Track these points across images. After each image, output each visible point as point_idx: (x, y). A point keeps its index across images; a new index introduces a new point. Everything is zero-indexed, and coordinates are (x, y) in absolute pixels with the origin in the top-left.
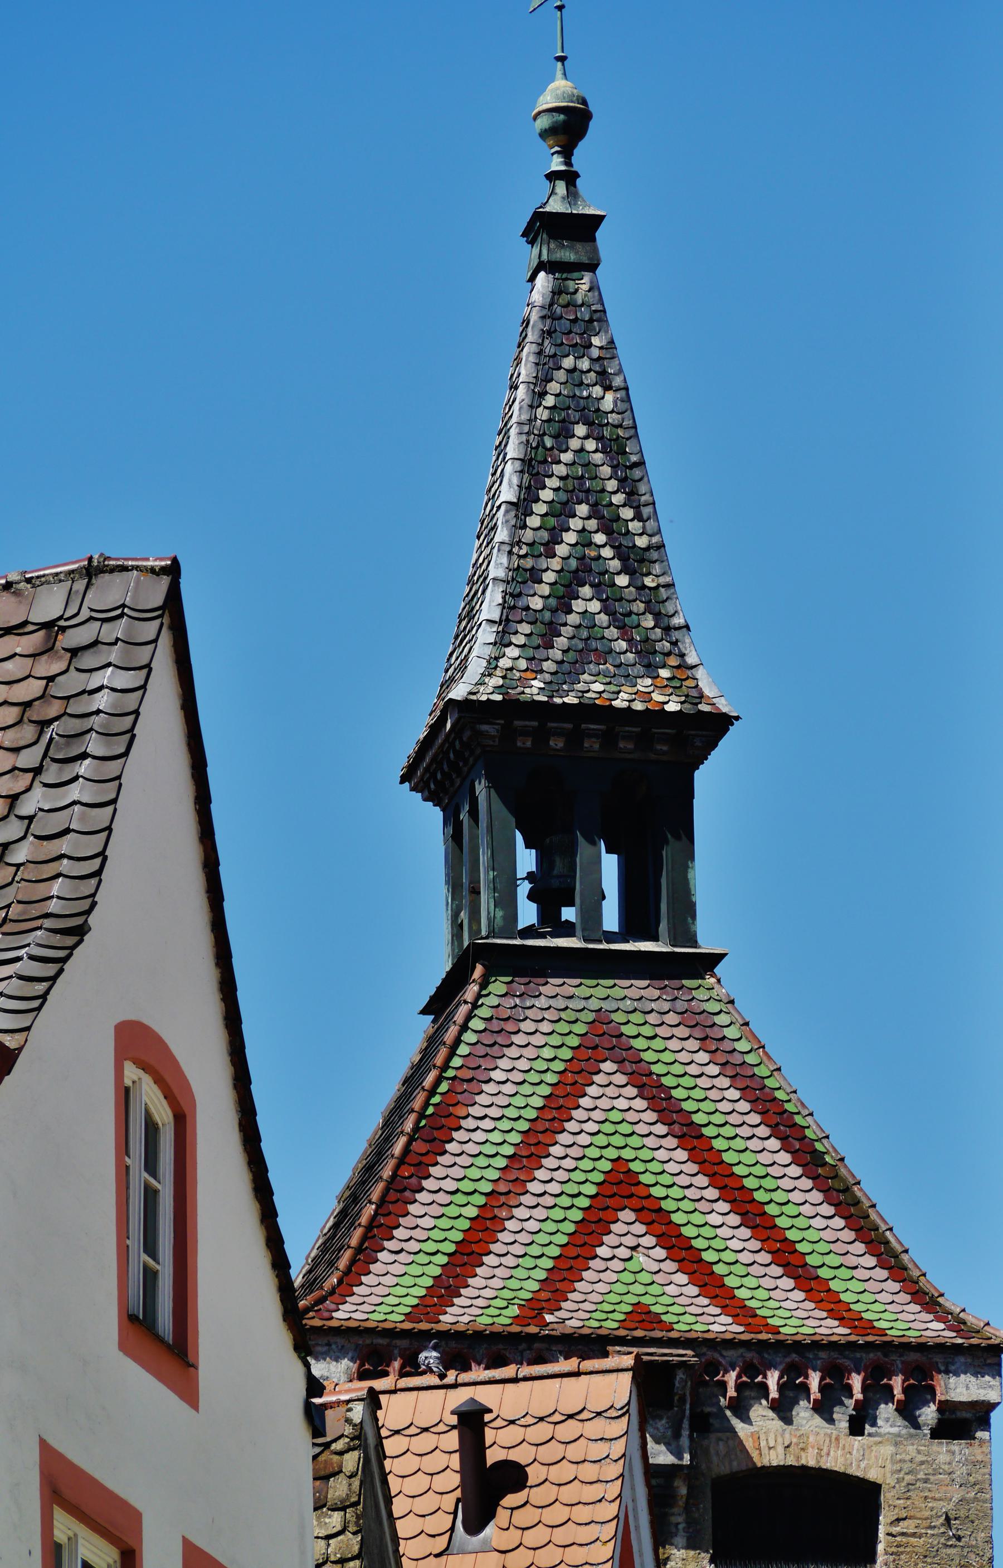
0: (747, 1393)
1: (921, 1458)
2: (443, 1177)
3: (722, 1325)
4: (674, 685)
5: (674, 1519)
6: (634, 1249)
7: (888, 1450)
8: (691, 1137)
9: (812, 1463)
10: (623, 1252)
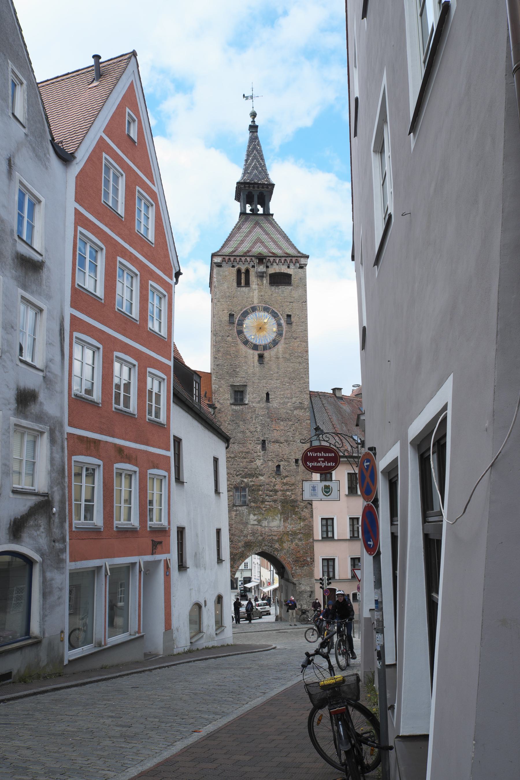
4: (267, 181)
7: (292, 270)
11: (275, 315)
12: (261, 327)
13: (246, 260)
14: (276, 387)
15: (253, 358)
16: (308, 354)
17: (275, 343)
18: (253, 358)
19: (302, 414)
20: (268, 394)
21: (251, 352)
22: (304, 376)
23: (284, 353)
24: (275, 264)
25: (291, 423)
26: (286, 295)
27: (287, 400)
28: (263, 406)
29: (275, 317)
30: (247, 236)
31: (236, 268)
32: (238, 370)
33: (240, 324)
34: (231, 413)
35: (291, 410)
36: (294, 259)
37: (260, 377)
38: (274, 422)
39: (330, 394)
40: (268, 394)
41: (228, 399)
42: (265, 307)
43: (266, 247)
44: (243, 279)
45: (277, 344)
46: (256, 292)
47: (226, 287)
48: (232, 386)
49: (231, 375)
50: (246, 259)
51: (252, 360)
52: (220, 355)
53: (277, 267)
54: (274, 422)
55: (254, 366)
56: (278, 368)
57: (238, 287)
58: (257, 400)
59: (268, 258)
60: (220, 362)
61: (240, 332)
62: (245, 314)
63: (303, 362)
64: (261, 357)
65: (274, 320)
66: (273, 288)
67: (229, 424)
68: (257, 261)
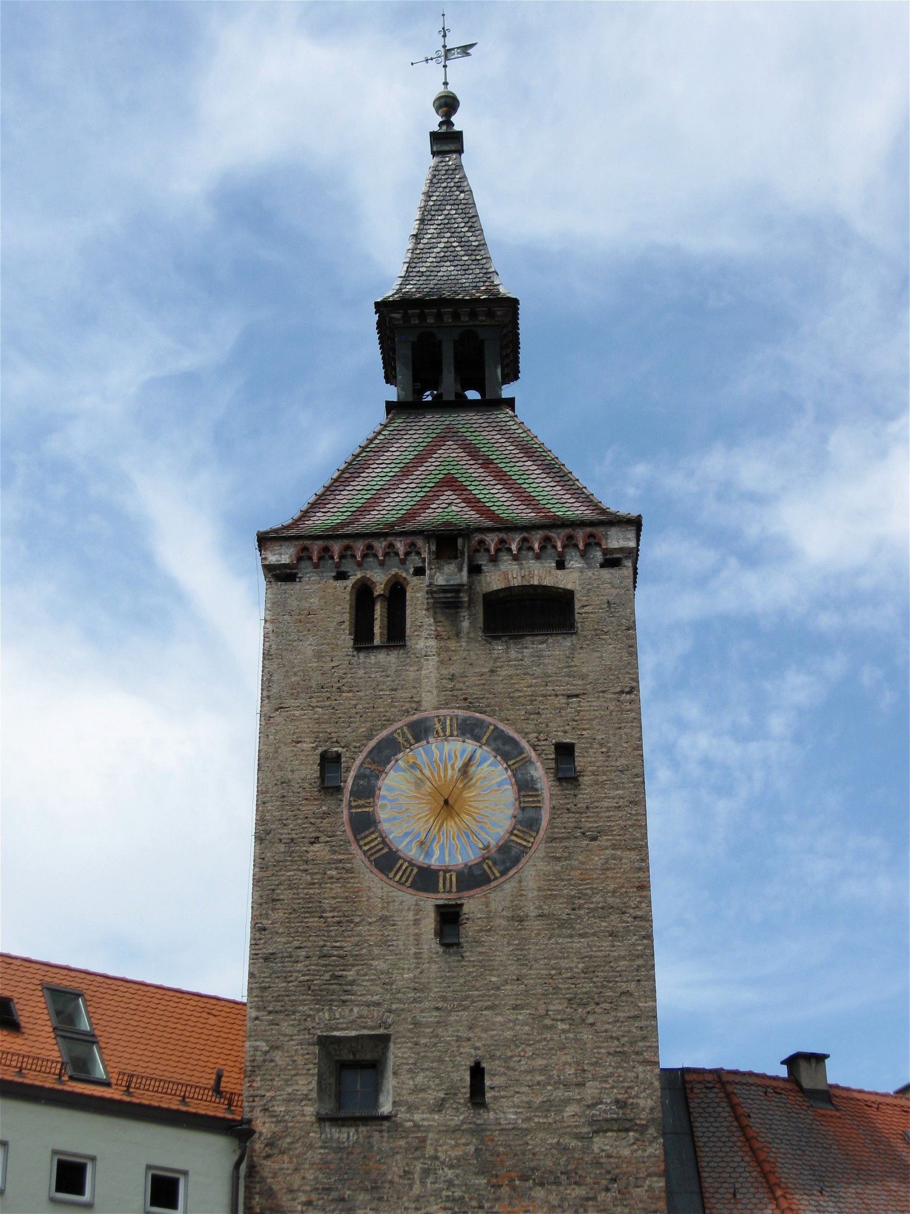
0: (501, 554)
1: (595, 577)
2: (358, 484)
3: (489, 524)
6: (449, 504)
7: (576, 575)
8: (487, 463)
9: (536, 583)
10: (444, 506)
11: (507, 749)
12: (446, 801)
13: (391, 551)
14: (515, 1041)
16: (647, 900)
17: (507, 857)
18: (417, 922)
19: (626, 1152)
20: (477, 1072)
21: (408, 897)
22: (632, 986)
23: (548, 896)
24: (505, 557)
25: (580, 1191)
26: (550, 669)
27: (560, 1094)
28: (457, 1120)
29: (506, 757)
30: (406, 471)
31: (349, 583)
32: (351, 974)
33: (366, 790)
34: (315, 1155)
35: (579, 1137)
36: (580, 535)
37: (444, 999)
38: (505, 1191)
39: (776, 1078)
40: (477, 1072)
41: (306, 1097)
42: (465, 720)
43: (473, 502)
44: (377, 620)
45: (516, 861)
46: (430, 667)
47: (309, 652)
48: (325, 1043)
49: (322, 998)
50: (391, 546)
51: (412, 930)
52: (280, 915)
53: (515, 567)
54: (505, 1191)
55: (418, 956)
56: (522, 961)
57: (358, 649)
58: (432, 1096)
59: (478, 537)
60: (279, 944)
61: (364, 823)
62: (385, 753)
63: (627, 930)
64: (449, 919)
65: (501, 768)
66: (499, 648)
67: (309, 1203)
68: (434, 548)
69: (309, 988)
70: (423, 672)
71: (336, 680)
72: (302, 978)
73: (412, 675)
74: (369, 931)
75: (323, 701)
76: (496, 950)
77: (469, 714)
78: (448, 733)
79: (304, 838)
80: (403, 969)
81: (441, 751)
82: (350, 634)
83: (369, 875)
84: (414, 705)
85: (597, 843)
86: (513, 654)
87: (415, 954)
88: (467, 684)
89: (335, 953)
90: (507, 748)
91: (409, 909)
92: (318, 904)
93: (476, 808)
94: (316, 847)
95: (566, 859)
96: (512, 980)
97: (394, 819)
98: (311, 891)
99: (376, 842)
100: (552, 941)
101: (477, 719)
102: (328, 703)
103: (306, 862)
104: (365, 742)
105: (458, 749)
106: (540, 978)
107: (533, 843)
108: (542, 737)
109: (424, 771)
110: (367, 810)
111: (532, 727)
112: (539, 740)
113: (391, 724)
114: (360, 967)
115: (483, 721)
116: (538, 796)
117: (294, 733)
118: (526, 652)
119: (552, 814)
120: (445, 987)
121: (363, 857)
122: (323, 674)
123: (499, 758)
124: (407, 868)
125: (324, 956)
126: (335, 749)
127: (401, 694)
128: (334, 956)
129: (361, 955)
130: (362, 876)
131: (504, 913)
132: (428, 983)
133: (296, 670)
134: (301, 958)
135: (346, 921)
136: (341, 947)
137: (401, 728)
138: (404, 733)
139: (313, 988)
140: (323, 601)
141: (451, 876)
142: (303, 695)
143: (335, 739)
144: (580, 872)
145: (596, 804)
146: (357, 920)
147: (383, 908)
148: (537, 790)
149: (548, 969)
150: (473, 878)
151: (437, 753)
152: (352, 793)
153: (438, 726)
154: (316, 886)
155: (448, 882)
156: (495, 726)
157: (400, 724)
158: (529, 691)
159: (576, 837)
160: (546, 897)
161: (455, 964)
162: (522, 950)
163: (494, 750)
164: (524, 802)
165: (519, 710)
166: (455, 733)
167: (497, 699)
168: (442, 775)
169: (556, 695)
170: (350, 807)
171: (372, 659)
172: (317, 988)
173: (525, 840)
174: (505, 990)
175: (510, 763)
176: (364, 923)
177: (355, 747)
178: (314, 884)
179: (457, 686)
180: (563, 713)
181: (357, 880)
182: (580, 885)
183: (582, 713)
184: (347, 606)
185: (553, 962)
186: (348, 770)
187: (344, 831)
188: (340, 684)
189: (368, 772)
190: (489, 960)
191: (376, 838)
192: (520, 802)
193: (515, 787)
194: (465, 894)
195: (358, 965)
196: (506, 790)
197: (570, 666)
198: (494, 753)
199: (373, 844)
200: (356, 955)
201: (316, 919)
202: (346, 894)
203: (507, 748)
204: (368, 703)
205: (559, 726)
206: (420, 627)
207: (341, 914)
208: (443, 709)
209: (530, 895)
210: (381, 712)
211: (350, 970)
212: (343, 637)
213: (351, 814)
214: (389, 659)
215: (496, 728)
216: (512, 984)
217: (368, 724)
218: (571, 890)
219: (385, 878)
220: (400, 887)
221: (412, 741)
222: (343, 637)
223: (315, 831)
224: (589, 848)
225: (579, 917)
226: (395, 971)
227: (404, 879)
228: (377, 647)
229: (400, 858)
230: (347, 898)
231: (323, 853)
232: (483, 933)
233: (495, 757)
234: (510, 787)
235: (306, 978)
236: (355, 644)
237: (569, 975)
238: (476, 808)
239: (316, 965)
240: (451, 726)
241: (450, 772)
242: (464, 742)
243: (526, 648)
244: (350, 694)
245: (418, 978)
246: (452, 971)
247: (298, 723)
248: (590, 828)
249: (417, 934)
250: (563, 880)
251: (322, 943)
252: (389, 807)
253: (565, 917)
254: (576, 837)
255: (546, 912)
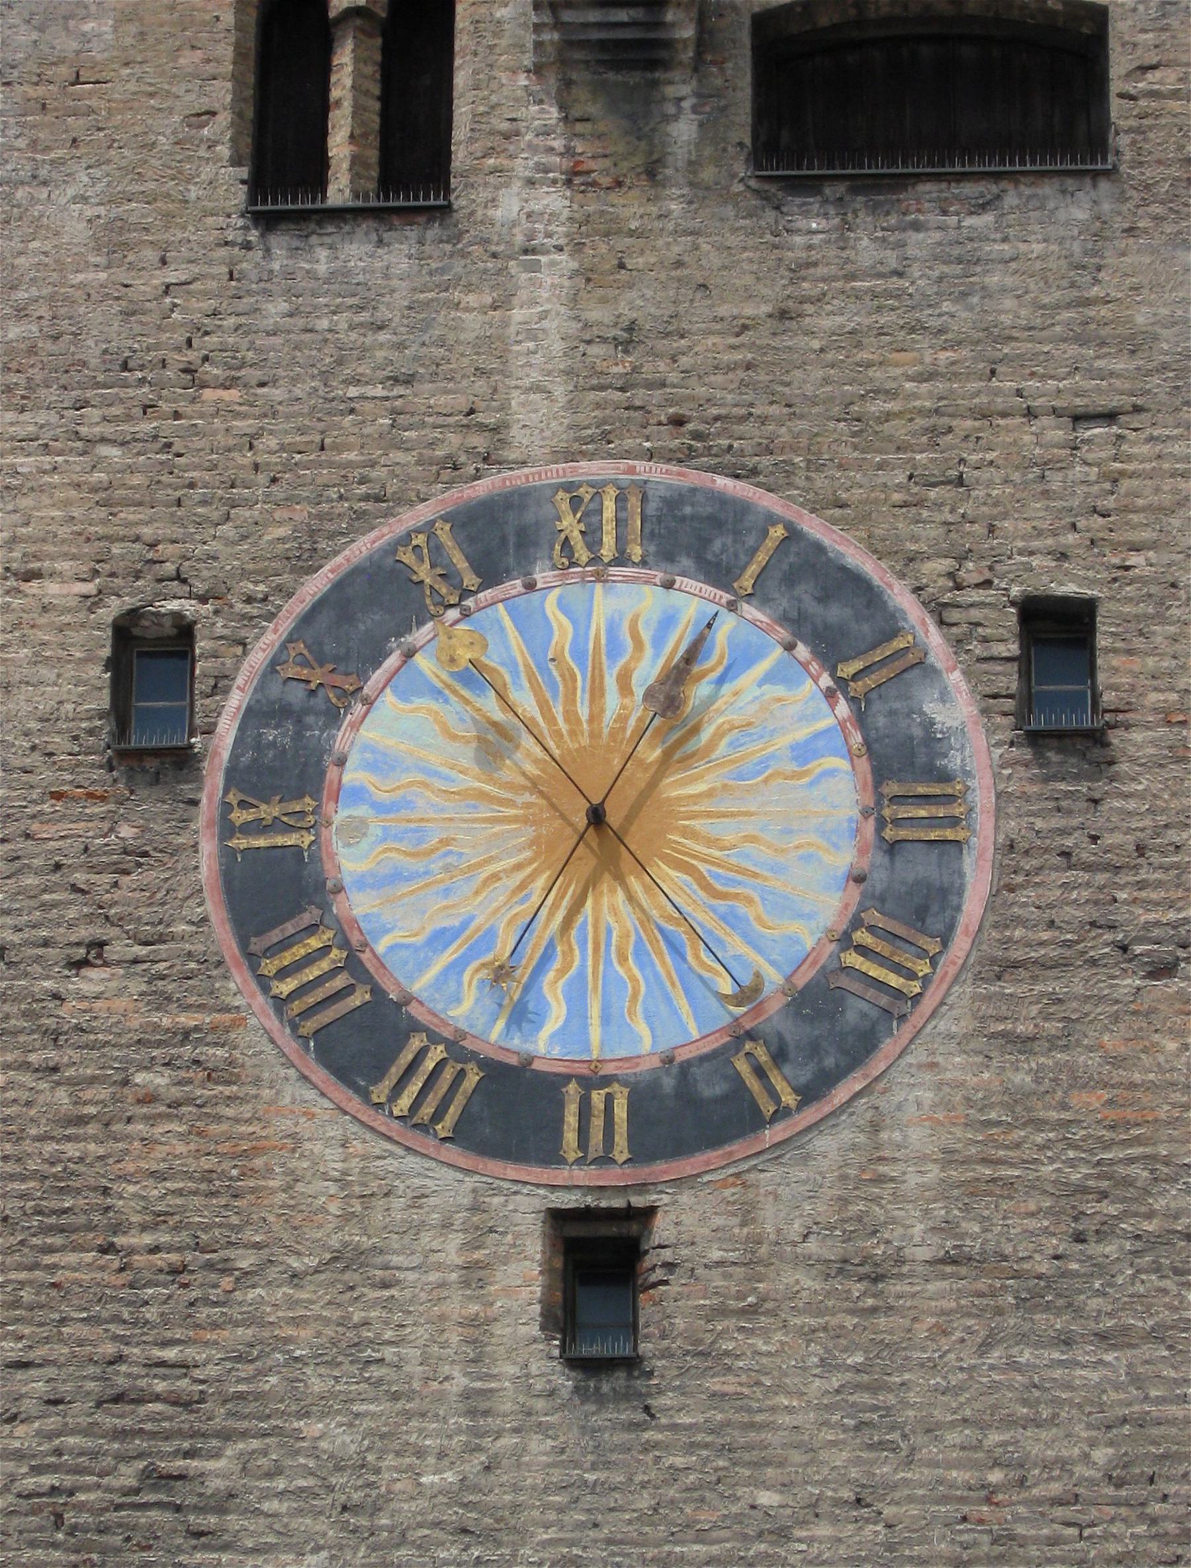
5: (670, 91)
11: (834, 619)
15: (475, 1275)
18: (475, 1275)
21: (444, 1180)
23: (978, 1182)
29: (829, 647)
32: (218, 1469)
33: (290, 766)
42: (674, 502)
45: (861, 1047)
47: (76, 230)
51: (457, 1306)
55: (476, 1404)
56: (875, 1431)
57: (267, 222)
61: (279, 894)
62: (365, 622)
65: (809, 689)
66: (812, 224)
69: (59, 1517)
70: (518, 315)
71: (179, 337)
72: (30, 1483)
73: (473, 324)
74: (293, 1303)
75: (128, 418)
76: (779, 1388)
77: (693, 478)
78: (608, 550)
79: (46, 943)
80: (420, 1453)
81: (580, 619)
82: (236, 161)
83: (293, 1091)
84: (479, 441)
85: (1174, 985)
86: (866, 248)
87: (466, 1395)
88: (685, 361)
89: (160, 1386)
90: (836, 613)
91: (446, 1225)
92: (98, 1199)
93: (711, 842)
94: (94, 980)
95: (1053, 1043)
96: (838, 1502)
97: (397, 877)
98: (72, 1150)
99: (325, 965)
100: (995, 1356)
101: (722, 500)
102: (146, 427)
103: (54, 1037)
104: (286, 578)
105: (646, 611)
106: (944, 1500)
107: (926, 980)
108: (971, 571)
109: (514, 695)
110: (291, 840)
111: (934, 532)
112: (959, 587)
113: (387, 514)
114: (255, 1444)
115: (743, 509)
116: (950, 799)
117: (14, 540)
118: (919, 243)
119: (1000, 869)
120: (580, 1526)
121: (273, 1023)
122: (128, 314)
123: (802, 651)
124: (440, 1065)
125: (118, 1399)
126: (173, 605)
127: (425, 396)
128: (157, 1398)
129: (259, 1396)
130: (266, 1093)
131: (812, 1246)
132: (516, 1508)
133: (21, 295)
134: (28, 1406)
135: (201, 1266)
136: (184, 1366)
137: (428, 528)
138: (437, 549)
139: (70, 1517)
140: (133, 28)
141: (609, 1099)
142: (51, 395)
143: (169, 568)
144: (1106, 1095)
145: (1173, 836)
146: (246, 1261)
147: (347, 1217)
148: (945, 777)
149: (975, 1465)
150: (693, 1111)
151: (562, 628)
152: (233, 775)
153: (570, 524)
154: (92, 1129)
155: (598, 1123)
156: (790, 528)
157: (424, 512)
158: (924, 395)
159: (1093, 962)
160: (973, 1189)
161: (621, 1437)
162: (874, 1388)
163: (784, 619)
164: (897, 822)
165: (881, 466)
166: (636, 552)
167: (801, 425)
168: (583, 712)
169: (1030, 413)
170: (228, 829)
171: (322, 260)
172: (85, 1518)
173: (897, 968)
174: (810, 1541)
175: (847, 670)
176: (273, 1273)
177: (249, 600)
178: (82, 1120)
179: (648, 371)
180: (1055, 481)
181: (246, 1111)
182: (1107, 1146)
183: (1125, 485)
184: (226, 51)
185: (994, 1437)
186: (220, 685)
187: (204, 920)
188: (193, 356)
189: (296, 695)
190: (752, 1426)
191: (325, 950)
192: (881, 823)
193: (864, 765)
194: (663, 1169)
195: (244, 1435)
196: (831, 773)
197: (1088, 302)
198: (783, 633)
199: (312, 973)
200: (241, 1396)
201: (89, 1257)
202: (206, 1163)
203: (836, 613)
204: (302, 431)
205: (1039, 533)
206: (507, 136)
207: (184, 1237)
208: (591, 456)
209: (913, 1180)
210: (350, 464)
211: (216, 1455)
212: (207, 172)
213: (228, 855)
214: (385, 262)
215: (793, 534)
216: (835, 1520)
217: (301, 513)
218: (1072, 1163)
219: (354, 1103)
220: (414, 1139)
221: (470, 580)
222: (207, 172)
223: (90, 919)
224: (1146, 1003)
225: (1100, 1268)
226: (390, 1461)
227: (427, 1110)
228: (339, 215)
229: (416, 1027)
230: (207, 1176)
231: (121, 1004)
232: (731, 1323)
233: (790, 647)
234: (843, 764)
235: (47, 1480)
236: (252, 199)
237: (1056, 1488)
238: (711, 842)
239: (86, 1432)
240: (619, 522)
241: (612, 701)
242: (669, 585)
243: (917, 227)
244: (233, 395)
245: (475, 1489)
246: (608, 1465)
247: (25, 502)
248: (1147, 926)
249: (472, 1322)
250: (1039, 1124)
251: (110, 1349)
252: (375, 830)
253: (1043, 1268)
254: (1093, 962)
255: (973, 1246)
